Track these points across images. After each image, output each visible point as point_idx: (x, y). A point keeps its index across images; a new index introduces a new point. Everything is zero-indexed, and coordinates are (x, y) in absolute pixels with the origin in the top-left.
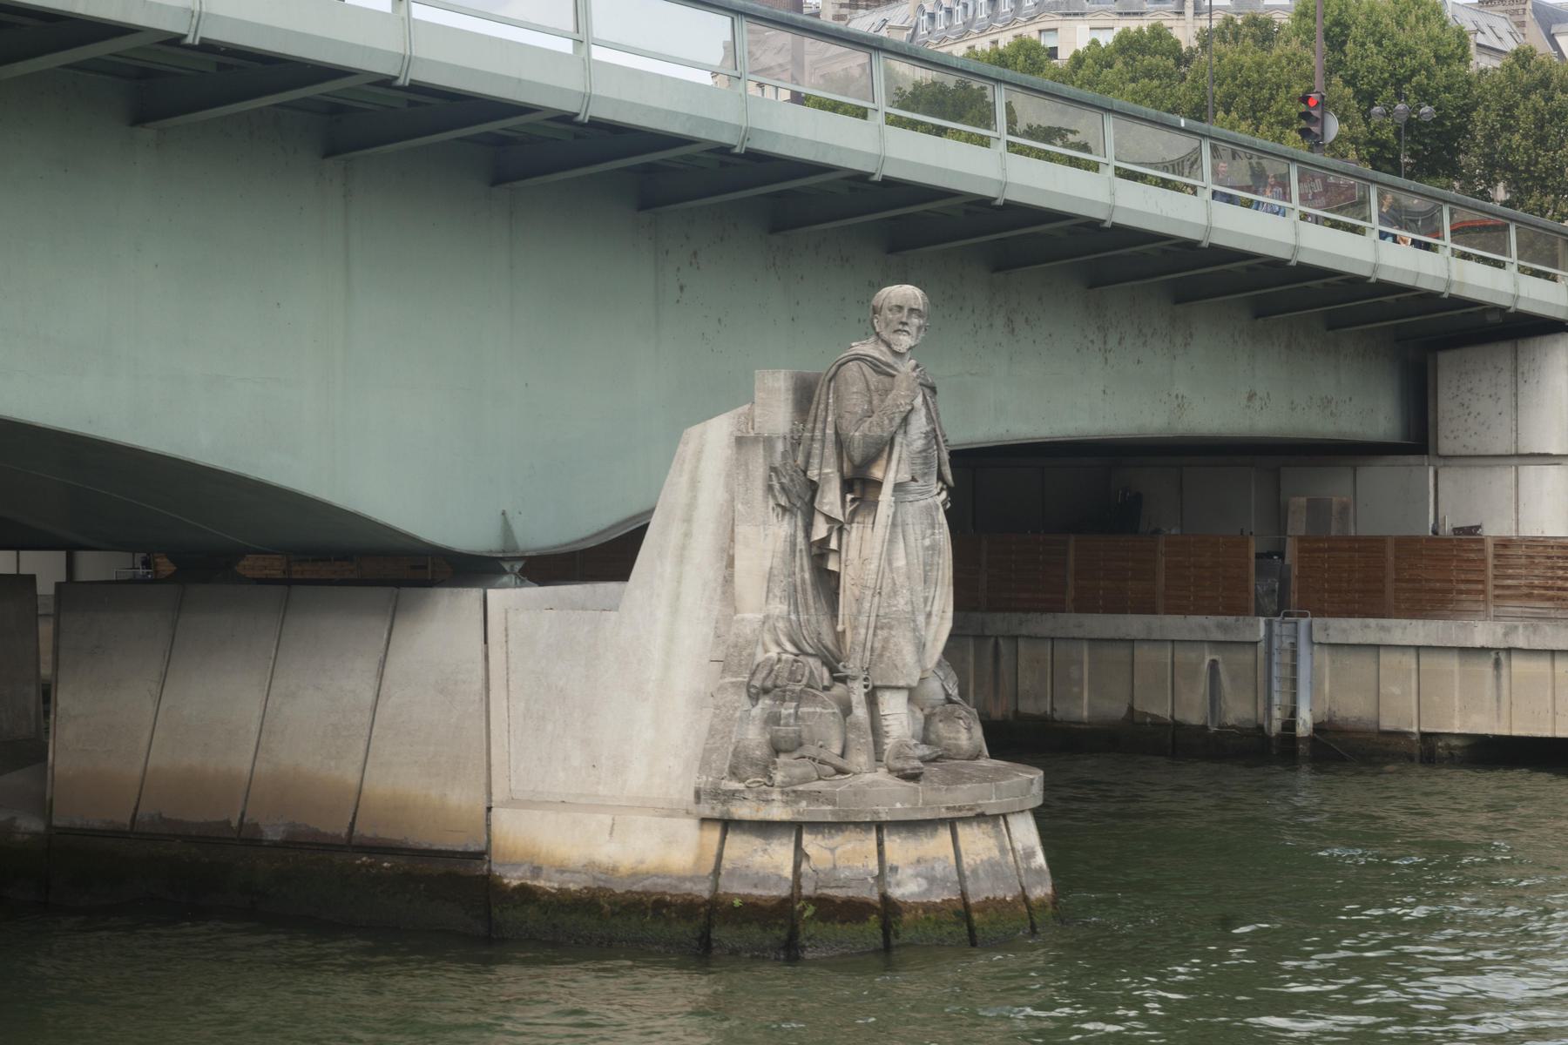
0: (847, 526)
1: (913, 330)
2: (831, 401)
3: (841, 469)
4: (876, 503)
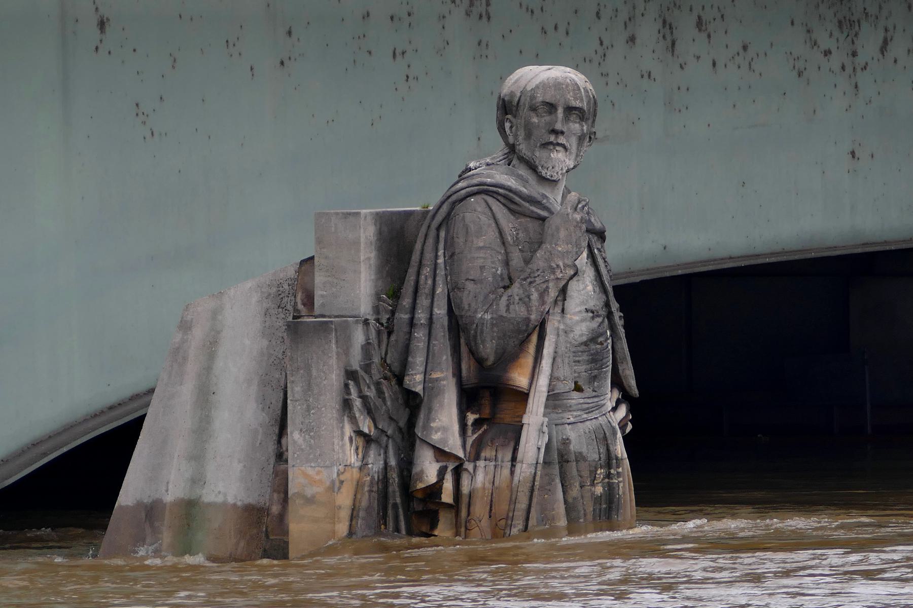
0: (469, 466)
1: (573, 143)
2: (441, 261)
3: (458, 374)
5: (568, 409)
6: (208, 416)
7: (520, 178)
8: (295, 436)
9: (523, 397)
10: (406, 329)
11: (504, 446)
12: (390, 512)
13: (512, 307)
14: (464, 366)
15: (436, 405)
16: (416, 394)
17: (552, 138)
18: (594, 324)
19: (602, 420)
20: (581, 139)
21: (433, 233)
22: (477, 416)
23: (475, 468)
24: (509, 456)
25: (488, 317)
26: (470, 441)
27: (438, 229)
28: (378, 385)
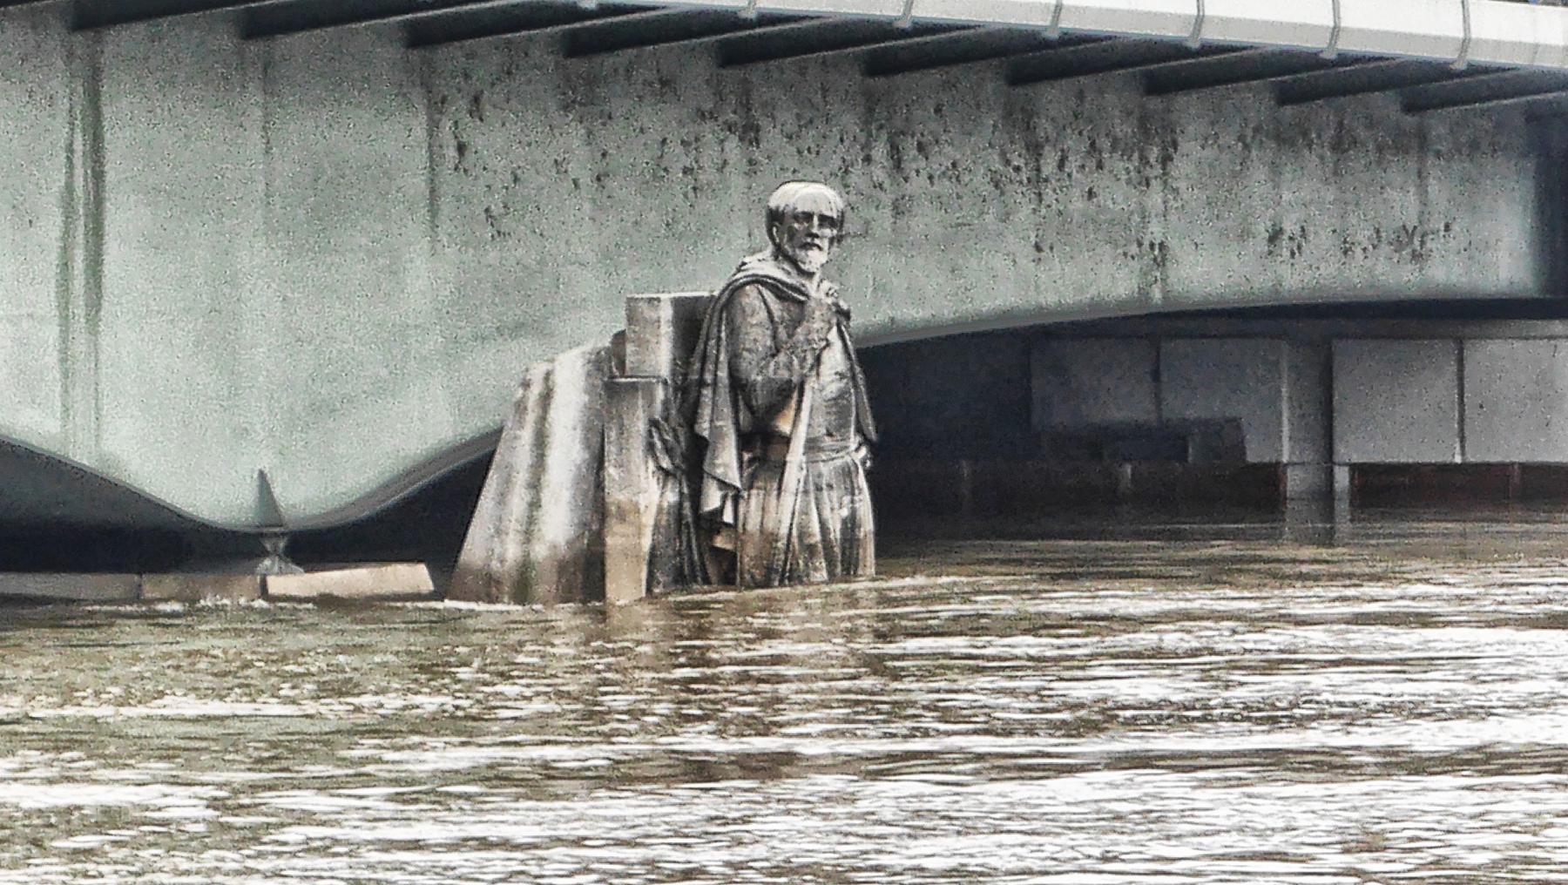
0: (745, 494)
1: (825, 244)
2: (723, 335)
3: (737, 423)
4: (783, 465)
5: (821, 449)
8: (611, 471)
9: (786, 441)
11: (772, 478)
14: (741, 417)
16: (703, 438)
17: (809, 240)
18: (842, 384)
19: (848, 459)
20: (832, 240)
21: (716, 314)
23: (749, 495)
24: (775, 486)
25: (759, 378)
26: (745, 475)
28: (674, 430)
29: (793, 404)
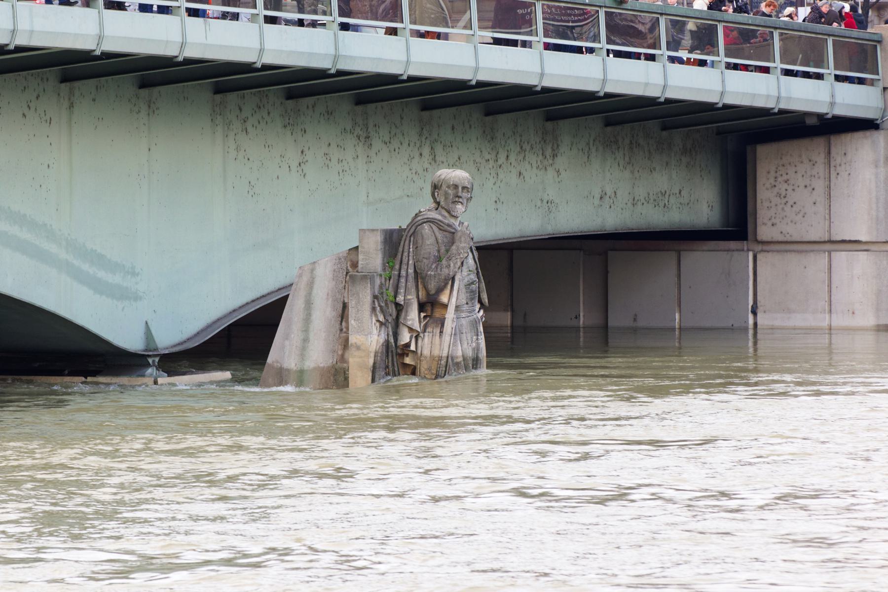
0: (422, 335)
2: (411, 250)
3: (418, 297)
5: (463, 311)
6: (310, 313)
7: (442, 216)
9: (445, 306)
10: (397, 278)
11: (436, 327)
12: (390, 354)
13: (443, 270)
14: (420, 294)
15: (409, 310)
16: (401, 305)
17: (457, 199)
19: (475, 316)
20: (468, 200)
22: (425, 314)
23: (424, 336)
27: (410, 237)
29: (449, 287)
